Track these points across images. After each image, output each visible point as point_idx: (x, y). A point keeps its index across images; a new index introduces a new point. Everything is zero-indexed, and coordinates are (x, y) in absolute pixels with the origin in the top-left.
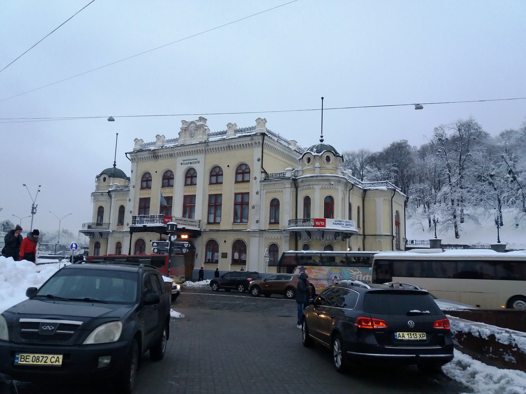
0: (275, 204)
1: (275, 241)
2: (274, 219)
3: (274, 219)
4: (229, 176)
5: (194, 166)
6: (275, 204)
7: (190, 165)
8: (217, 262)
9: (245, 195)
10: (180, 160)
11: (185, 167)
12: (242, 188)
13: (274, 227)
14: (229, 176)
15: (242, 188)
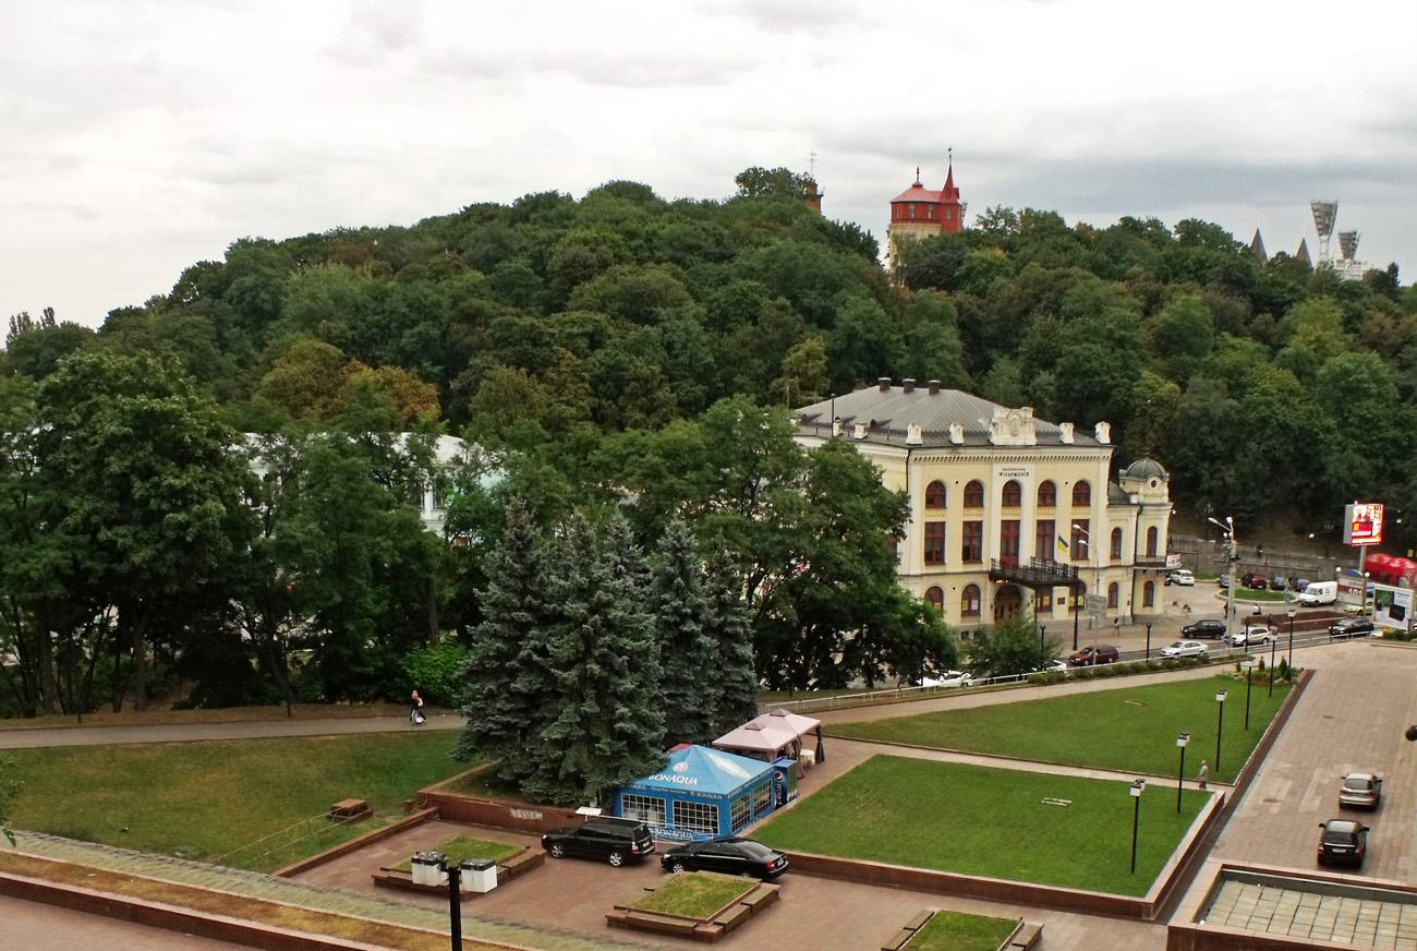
0: (1117, 535)
1: (1115, 579)
2: (1116, 554)
3: (1116, 554)
4: (1065, 495)
5: (1021, 479)
6: (1117, 535)
7: (1013, 478)
8: (1049, 609)
9: (1085, 524)
10: (998, 468)
11: (1009, 479)
12: (1081, 513)
13: (1116, 563)
14: (1065, 495)
15: (1081, 513)
